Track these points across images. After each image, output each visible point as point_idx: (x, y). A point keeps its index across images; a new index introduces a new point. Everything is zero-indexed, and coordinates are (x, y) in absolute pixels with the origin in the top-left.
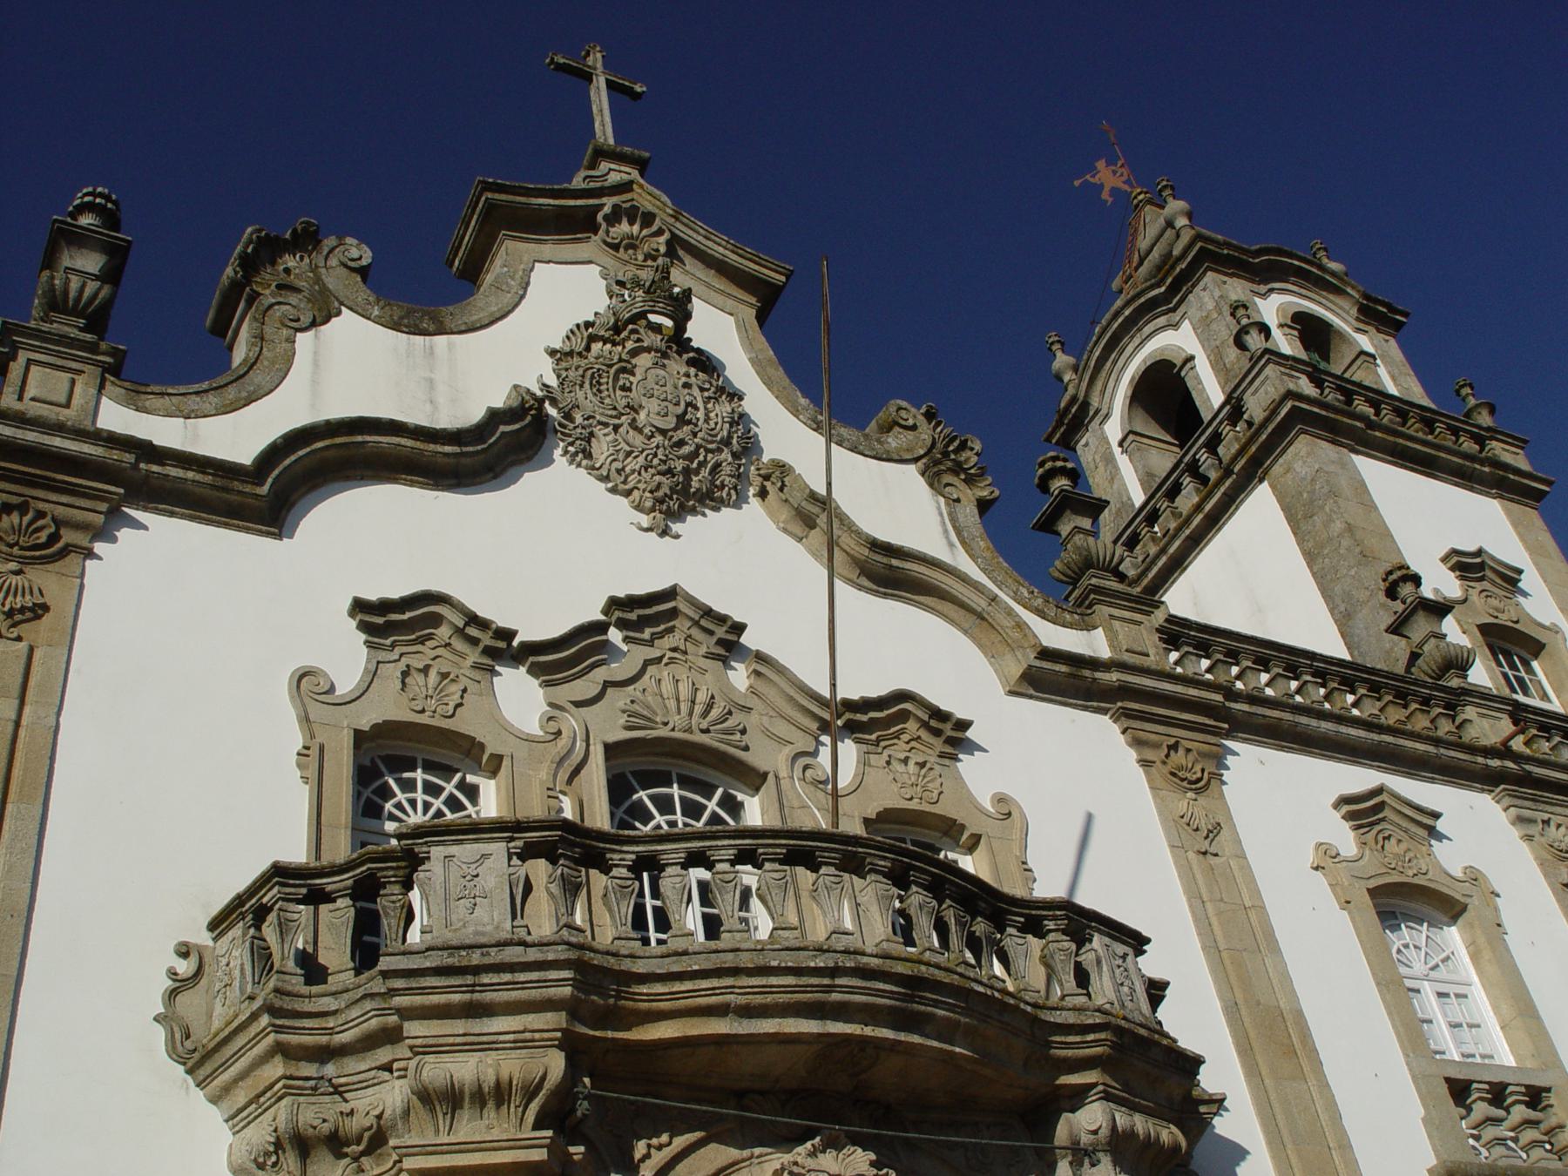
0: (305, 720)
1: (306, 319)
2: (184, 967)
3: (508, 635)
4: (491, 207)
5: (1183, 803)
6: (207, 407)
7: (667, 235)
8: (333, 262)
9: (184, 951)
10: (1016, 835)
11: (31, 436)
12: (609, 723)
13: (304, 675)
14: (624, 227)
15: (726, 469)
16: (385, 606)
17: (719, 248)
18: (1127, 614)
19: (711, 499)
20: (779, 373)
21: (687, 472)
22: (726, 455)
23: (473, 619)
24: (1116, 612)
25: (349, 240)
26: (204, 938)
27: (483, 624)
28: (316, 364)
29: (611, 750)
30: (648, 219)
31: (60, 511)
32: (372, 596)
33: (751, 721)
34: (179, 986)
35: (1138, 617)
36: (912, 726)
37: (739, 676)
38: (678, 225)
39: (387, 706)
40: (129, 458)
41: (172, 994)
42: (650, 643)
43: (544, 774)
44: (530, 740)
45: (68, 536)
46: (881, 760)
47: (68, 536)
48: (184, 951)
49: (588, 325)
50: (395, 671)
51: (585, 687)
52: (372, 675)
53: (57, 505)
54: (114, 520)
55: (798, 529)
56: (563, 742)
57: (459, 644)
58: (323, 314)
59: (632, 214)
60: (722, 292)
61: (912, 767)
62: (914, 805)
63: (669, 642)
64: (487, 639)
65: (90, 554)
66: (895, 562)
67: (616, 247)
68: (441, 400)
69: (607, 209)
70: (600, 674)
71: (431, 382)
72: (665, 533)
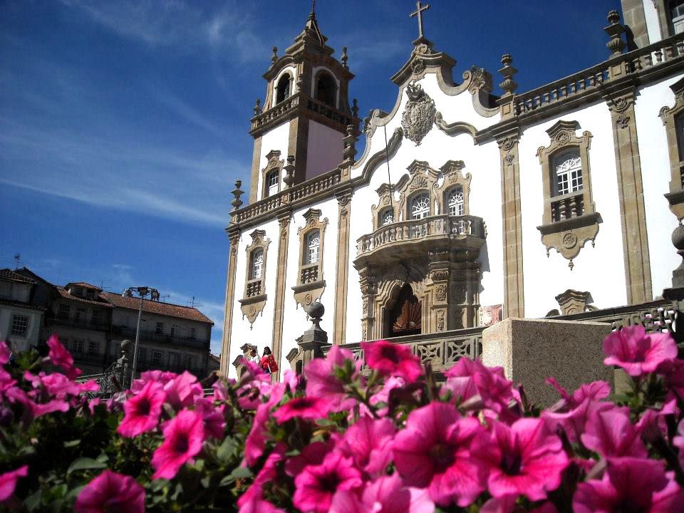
45: (349, 198)
65: (350, 200)
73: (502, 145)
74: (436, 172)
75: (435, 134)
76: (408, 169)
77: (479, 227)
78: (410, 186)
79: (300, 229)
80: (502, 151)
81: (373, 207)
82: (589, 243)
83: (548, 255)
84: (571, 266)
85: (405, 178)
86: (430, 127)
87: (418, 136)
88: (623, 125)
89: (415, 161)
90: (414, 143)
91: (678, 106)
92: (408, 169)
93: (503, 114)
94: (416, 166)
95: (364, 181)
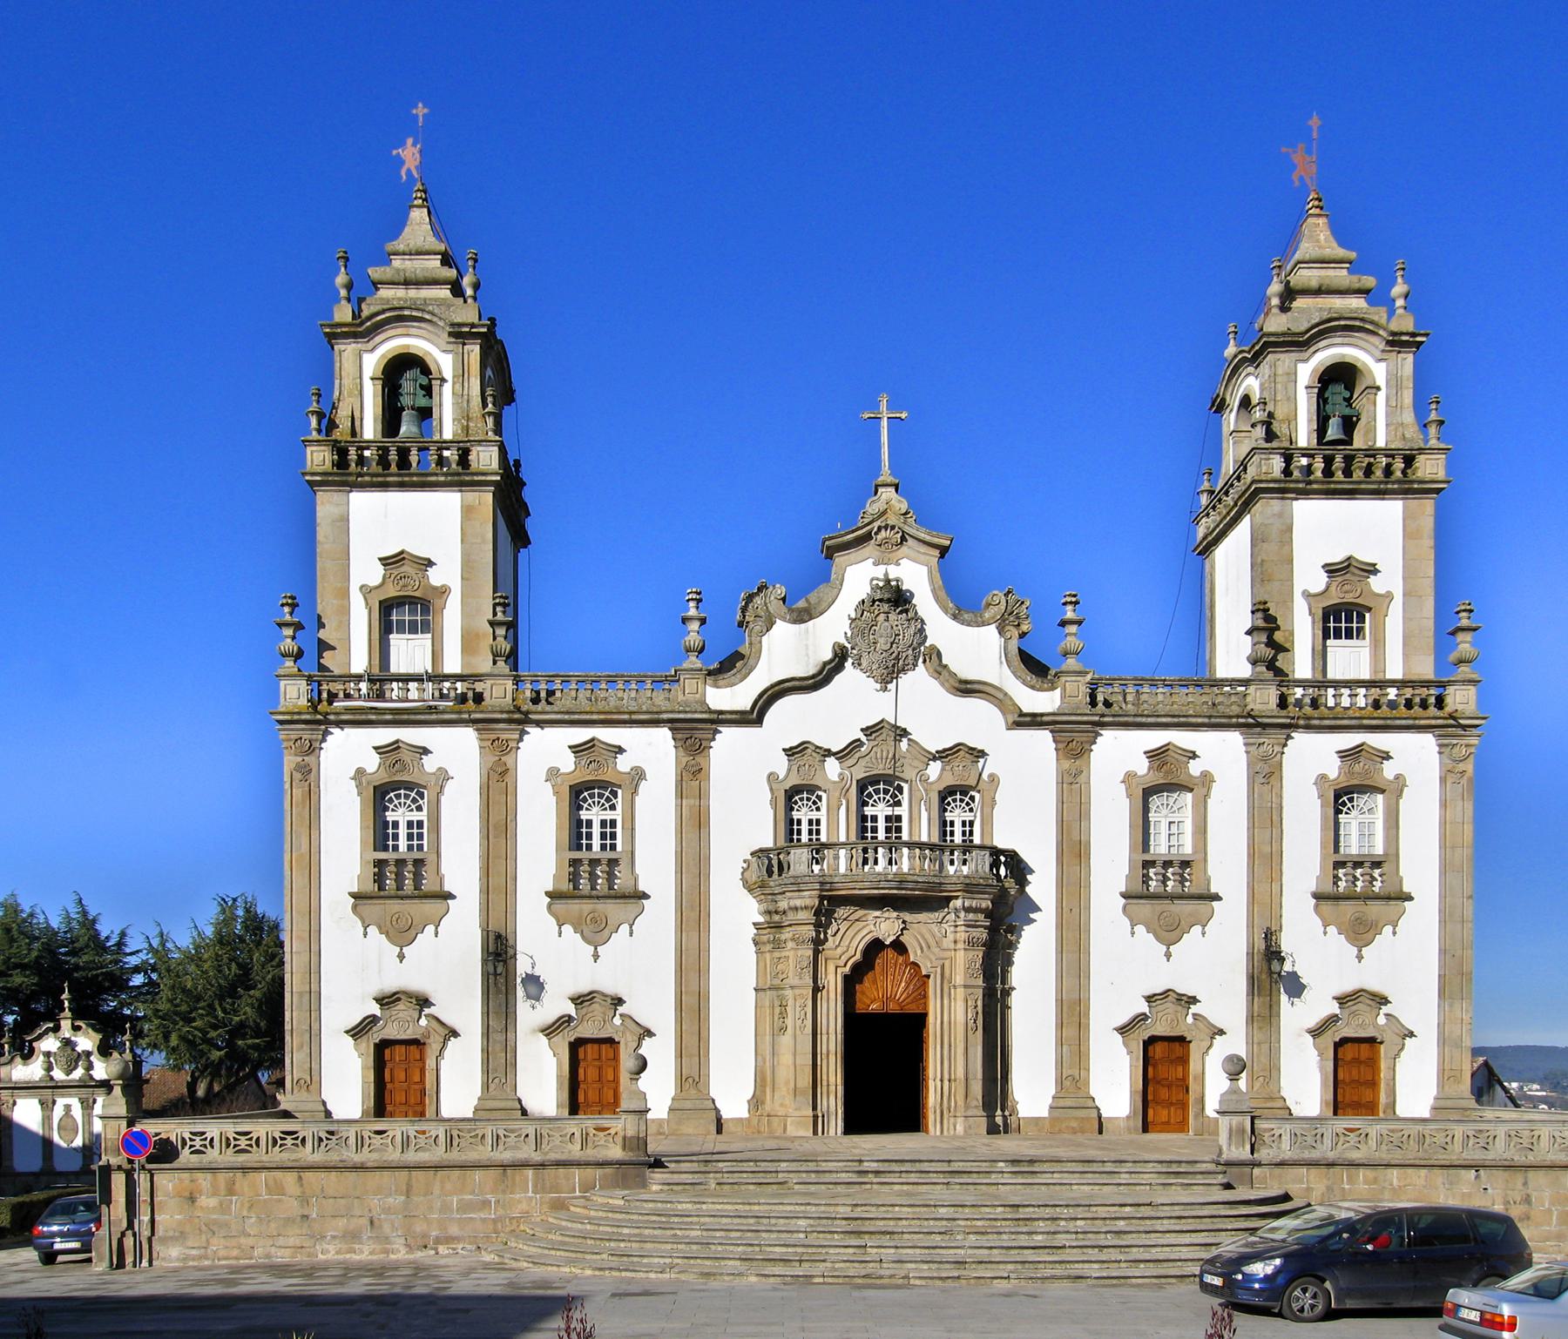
0: (771, 789)
1: (764, 631)
2: (745, 865)
3: (829, 750)
4: (828, 548)
5: (1066, 764)
6: (737, 680)
7: (900, 534)
8: (772, 598)
9: (745, 861)
10: (994, 788)
11: (689, 716)
12: (860, 773)
13: (770, 774)
14: (883, 534)
15: (910, 658)
16: (791, 748)
17: (922, 536)
18: (1074, 678)
19: (903, 670)
20: (942, 594)
21: (893, 666)
22: (910, 652)
23: (817, 747)
24: (1068, 679)
25: (778, 586)
26: (750, 857)
27: (821, 748)
28: (769, 650)
29: (858, 781)
30: (893, 528)
31: (700, 736)
32: (787, 747)
33: (905, 761)
34: (745, 870)
35: (1079, 678)
36: (961, 752)
37: (904, 744)
38: (906, 527)
39: (794, 780)
40: (716, 716)
41: (742, 873)
42: (875, 740)
43: (837, 794)
44: (835, 782)
46: (948, 768)
47: (704, 744)
48: (745, 861)
49: (863, 601)
50: (795, 768)
51: (851, 761)
52: (789, 770)
53: (698, 734)
54: (717, 732)
55: (936, 675)
56: (844, 782)
57: (814, 754)
58: (770, 625)
59: (886, 527)
60: (924, 554)
61: (961, 768)
62: (958, 783)
63: (881, 738)
64: (822, 753)
66: (969, 686)
67: (880, 545)
68: (810, 653)
69: (875, 529)
70: (857, 755)
71: (807, 645)
72: (885, 689)
73: (1061, 746)
74: (930, 753)
75: (918, 680)
76: (862, 730)
77: (1018, 868)
78: (863, 762)
79: (553, 774)
80: (1061, 757)
81: (772, 778)
82: (1197, 929)
83: (1133, 934)
84: (1168, 956)
85: (856, 744)
86: (915, 665)
87: (890, 673)
88: (1263, 780)
89: (882, 721)
90: (873, 685)
91: (1339, 780)
92: (862, 730)
93: (1063, 697)
94: (886, 732)
95: (753, 717)
